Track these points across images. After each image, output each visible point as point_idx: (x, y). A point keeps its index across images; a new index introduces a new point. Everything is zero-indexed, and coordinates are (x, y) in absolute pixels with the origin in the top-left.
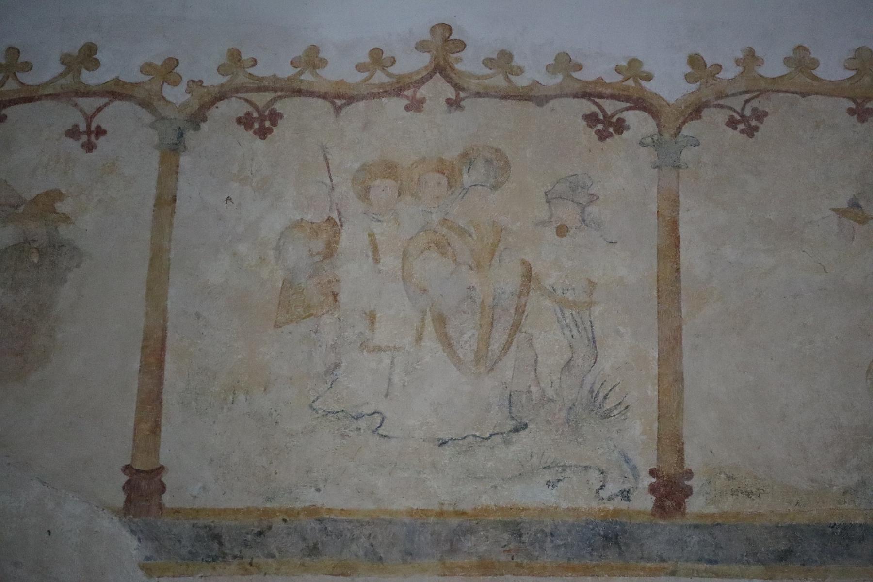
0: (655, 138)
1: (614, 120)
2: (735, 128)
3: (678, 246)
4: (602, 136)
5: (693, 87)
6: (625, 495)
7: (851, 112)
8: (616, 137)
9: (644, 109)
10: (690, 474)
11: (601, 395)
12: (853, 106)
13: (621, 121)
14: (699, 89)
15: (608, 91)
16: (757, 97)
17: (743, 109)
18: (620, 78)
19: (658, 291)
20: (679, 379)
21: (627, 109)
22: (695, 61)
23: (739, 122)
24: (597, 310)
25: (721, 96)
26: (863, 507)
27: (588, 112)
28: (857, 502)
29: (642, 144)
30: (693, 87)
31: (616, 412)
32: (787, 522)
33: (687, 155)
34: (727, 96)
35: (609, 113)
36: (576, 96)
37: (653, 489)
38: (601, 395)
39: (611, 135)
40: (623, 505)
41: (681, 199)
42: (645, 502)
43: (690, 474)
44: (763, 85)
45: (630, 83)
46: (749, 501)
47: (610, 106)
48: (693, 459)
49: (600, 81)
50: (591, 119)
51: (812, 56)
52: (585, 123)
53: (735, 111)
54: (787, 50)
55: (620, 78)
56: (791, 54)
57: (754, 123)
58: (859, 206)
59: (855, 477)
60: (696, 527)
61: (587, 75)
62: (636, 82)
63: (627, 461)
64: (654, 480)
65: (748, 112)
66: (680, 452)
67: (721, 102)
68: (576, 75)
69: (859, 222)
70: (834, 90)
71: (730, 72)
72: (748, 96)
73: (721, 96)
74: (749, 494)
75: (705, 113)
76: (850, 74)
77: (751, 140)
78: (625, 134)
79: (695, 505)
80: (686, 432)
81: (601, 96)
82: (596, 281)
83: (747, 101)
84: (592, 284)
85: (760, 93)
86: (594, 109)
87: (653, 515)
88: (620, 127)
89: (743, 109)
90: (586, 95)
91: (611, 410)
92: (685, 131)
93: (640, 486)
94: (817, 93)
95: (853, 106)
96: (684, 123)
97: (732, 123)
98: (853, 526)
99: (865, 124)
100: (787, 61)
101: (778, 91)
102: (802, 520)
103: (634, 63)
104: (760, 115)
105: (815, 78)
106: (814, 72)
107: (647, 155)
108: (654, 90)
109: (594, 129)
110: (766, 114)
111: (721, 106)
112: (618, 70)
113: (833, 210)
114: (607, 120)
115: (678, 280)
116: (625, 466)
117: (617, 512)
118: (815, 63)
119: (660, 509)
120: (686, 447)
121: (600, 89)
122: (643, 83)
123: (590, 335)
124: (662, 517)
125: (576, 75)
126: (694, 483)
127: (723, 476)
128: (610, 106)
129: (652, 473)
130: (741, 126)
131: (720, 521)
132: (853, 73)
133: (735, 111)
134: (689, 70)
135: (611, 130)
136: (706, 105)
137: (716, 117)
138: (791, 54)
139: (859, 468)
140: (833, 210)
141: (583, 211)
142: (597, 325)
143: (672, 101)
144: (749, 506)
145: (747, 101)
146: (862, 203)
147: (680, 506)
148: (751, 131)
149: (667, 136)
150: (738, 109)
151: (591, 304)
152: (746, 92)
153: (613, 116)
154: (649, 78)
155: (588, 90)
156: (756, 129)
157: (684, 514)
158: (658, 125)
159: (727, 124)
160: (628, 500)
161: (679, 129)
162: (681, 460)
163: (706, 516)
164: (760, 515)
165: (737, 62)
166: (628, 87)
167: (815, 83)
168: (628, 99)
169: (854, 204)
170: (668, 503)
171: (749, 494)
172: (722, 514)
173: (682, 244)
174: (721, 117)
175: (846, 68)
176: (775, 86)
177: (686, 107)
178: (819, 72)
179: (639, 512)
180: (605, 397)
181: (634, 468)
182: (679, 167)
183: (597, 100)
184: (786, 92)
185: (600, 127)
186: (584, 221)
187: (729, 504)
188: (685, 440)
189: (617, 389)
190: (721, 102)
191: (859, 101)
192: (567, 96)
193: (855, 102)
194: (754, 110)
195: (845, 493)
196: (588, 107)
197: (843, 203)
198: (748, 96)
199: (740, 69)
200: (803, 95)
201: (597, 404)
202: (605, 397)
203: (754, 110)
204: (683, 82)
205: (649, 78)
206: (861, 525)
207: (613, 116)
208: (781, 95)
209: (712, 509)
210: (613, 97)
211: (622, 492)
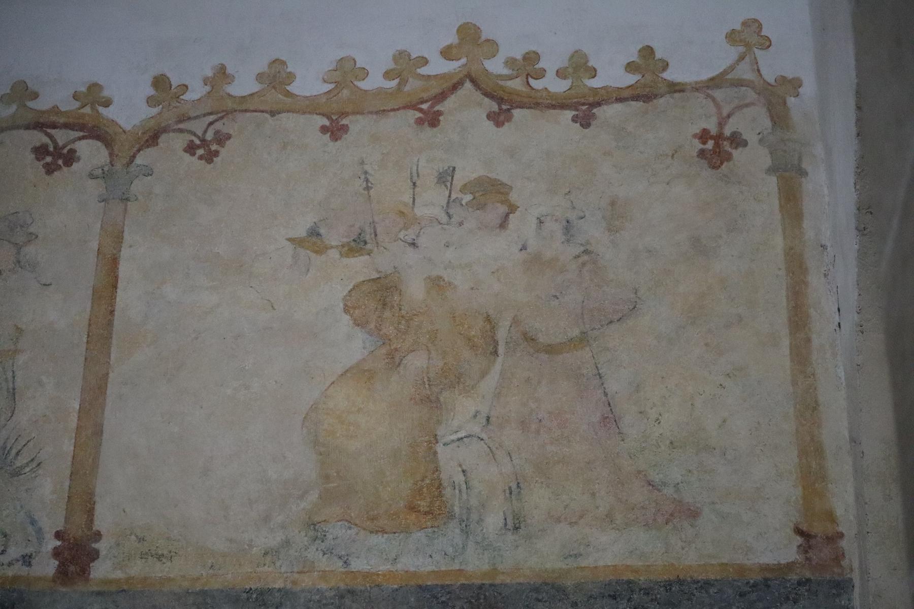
0: (106, 169)
1: (65, 151)
2: (193, 154)
3: (115, 287)
4: (50, 170)
5: (155, 111)
6: (27, 560)
7: (324, 129)
8: (65, 169)
9: (98, 138)
10: (98, 536)
11: (14, 452)
12: (326, 122)
13: (72, 151)
14: (159, 114)
15: (62, 120)
16: (222, 118)
17: (205, 132)
18: (77, 104)
19: (88, 336)
20: (99, 432)
21: (80, 139)
22: (160, 82)
23: (199, 147)
24: (21, 359)
25: (184, 118)
26: (283, 570)
27: (38, 144)
28: (278, 564)
29: (92, 176)
30: (155, 111)
31: (27, 469)
32: (198, 587)
33: (137, 187)
34: (189, 118)
35: (61, 144)
36: (27, 127)
37: (56, 553)
38: (14, 452)
39: (59, 168)
40: (23, 571)
41: (126, 235)
42: (47, 567)
43: (98, 536)
44: (230, 105)
45: (87, 110)
46: (158, 564)
47: (61, 136)
48: (104, 520)
49: (55, 110)
50: (40, 151)
51: (289, 70)
52: (33, 156)
53: (195, 135)
54: (261, 65)
55: (77, 104)
56: (266, 69)
57: (214, 147)
58: (318, 235)
59: (279, 537)
60: (99, 593)
61: (42, 104)
62: (93, 108)
63: (33, 522)
64: (59, 543)
65: (209, 136)
66: (90, 512)
67: (181, 126)
68: (31, 104)
69: (316, 252)
70: (310, 107)
71: (196, 92)
72: (211, 118)
73: (187, 118)
74: (160, 557)
75: (163, 138)
76: (331, 86)
77: (209, 167)
78: (75, 166)
79: (101, 570)
80: (98, 490)
81: (54, 126)
82: (24, 327)
83: (211, 124)
84: (19, 330)
85: (227, 113)
86: (46, 140)
87: (54, 581)
88: (70, 158)
89: (205, 132)
90: (39, 126)
91: (22, 467)
92: (139, 160)
93: (43, 549)
94: (288, 111)
95: (326, 122)
96: (139, 151)
97: (191, 149)
98: (270, 591)
99: (339, 142)
100: (260, 77)
101: (246, 111)
102: (215, 585)
103: (95, 87)
104: (222, 139)
105: (288, 94)
106: (288, 88)
107: (95, 188)
108: (111, 116)
109: (42, 163)
110: (229, 137)
111: (181, 131)
112: (76, 96)
113: (289, 240)
114: (57, 152)
115: (110, 324)
116: (30, 529)
117: (16, 579)
118: (291, 77)
119: (63, 575)
120: (98, 507)
121: (53, 118)
122: (101, 109)
123: (11, 386)
124: (64, 584)
125: (31, 104)
126: (102, 546)
127: (133, 537)
128: (61, 136)
129: (58, 535)
130: (200, 152)
131: (125, 587)
132: (331, 86)
133: (195, 135)
134: (151, 91)
135: (60, 162)
136: (165, 130)
137: (175, 142)
138: (266, 69)
139: (283, 527)
140: (289, 240)
141: (18, 253)
142: (19, 374)
143: (128, 127)
144: (158, 570)
145: (211, 124)
146: (322, 231)
147: (84, 572)
148: (210, 157)
149: (118, 166)
150: (200, 135)
151: (16, 352)
152: (211, 114)
153: (64, 147)
154: (107, 103)
155: (41, 120)
156: (216, 153)
157: (87, 580)
158: (111, 155)
159: (185, 151)
160: (30, 565)
161: (134, 157)
162: (90, 520)
163: (110, 582)
164: (169, 580)
165: (206, 81)
166: (84, 115)
167: (289, 100)
168: (82, 128)
169: (314, 233)
170: (72, 568)
171: (160, 557)
172: (129, 580)
173: (120, 285)
174: (178, 142)
175: (325, 81)
176: (243, 105)
177: (144, 133)
178: (293, 88)
179: (39, 579)
180: (17, 454)
181: (39, 531)
182: (127, 199)
183: (49, 131)
184: (255, 111)
185: (49, 159)
186: (19, 262)
187: (137, 569)
188: (97, 499)
189: (31, 444)
190: (181, 126)
191: (334, 118)
192: (18, 127)
193: (329, 118)
194: (217, 132)
195: (266, 554)
196: (39, 138)
197: (301, 232)
198: (211, 118)
199: (208, 88)
200: (273, 113)
201: (9, 460)
202: (17, 454)
203: (217, 132)
204: (144, 105)
205: (107, 103)
206: (279, 590)
207: (64, 147)
208: (248, 114)
209: (119, 574)
210: (66, 126)
211: (23, 557)
